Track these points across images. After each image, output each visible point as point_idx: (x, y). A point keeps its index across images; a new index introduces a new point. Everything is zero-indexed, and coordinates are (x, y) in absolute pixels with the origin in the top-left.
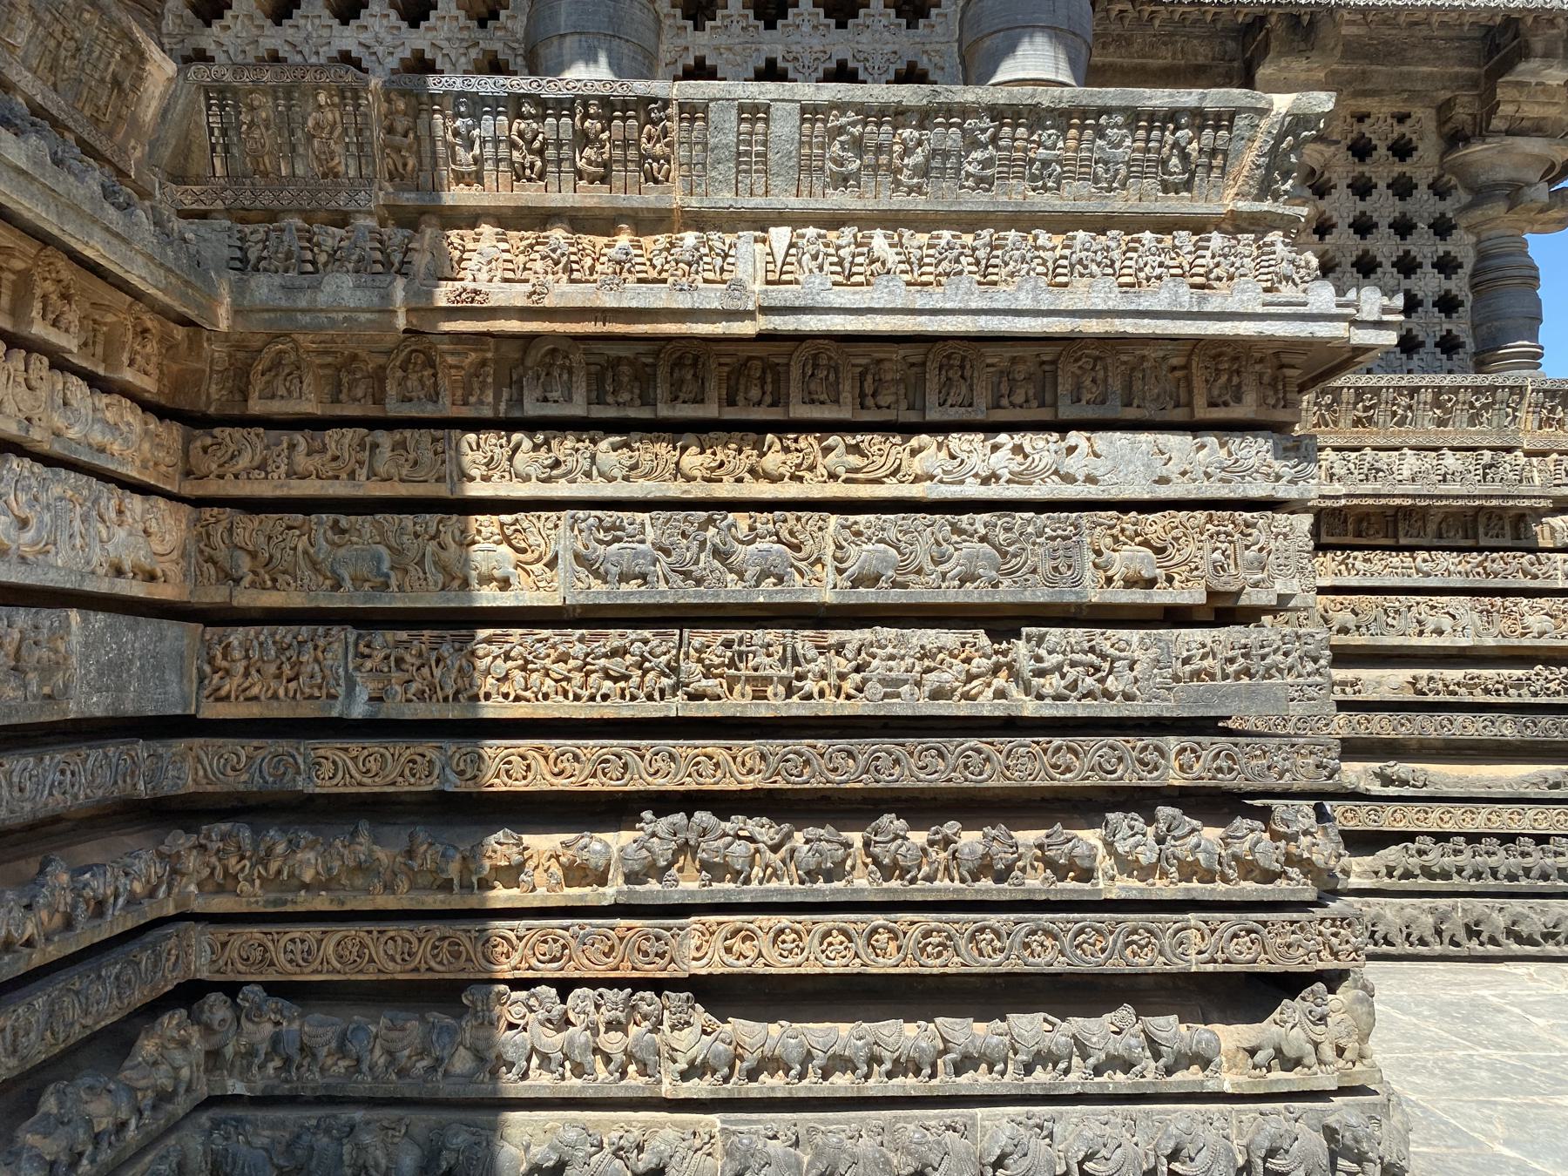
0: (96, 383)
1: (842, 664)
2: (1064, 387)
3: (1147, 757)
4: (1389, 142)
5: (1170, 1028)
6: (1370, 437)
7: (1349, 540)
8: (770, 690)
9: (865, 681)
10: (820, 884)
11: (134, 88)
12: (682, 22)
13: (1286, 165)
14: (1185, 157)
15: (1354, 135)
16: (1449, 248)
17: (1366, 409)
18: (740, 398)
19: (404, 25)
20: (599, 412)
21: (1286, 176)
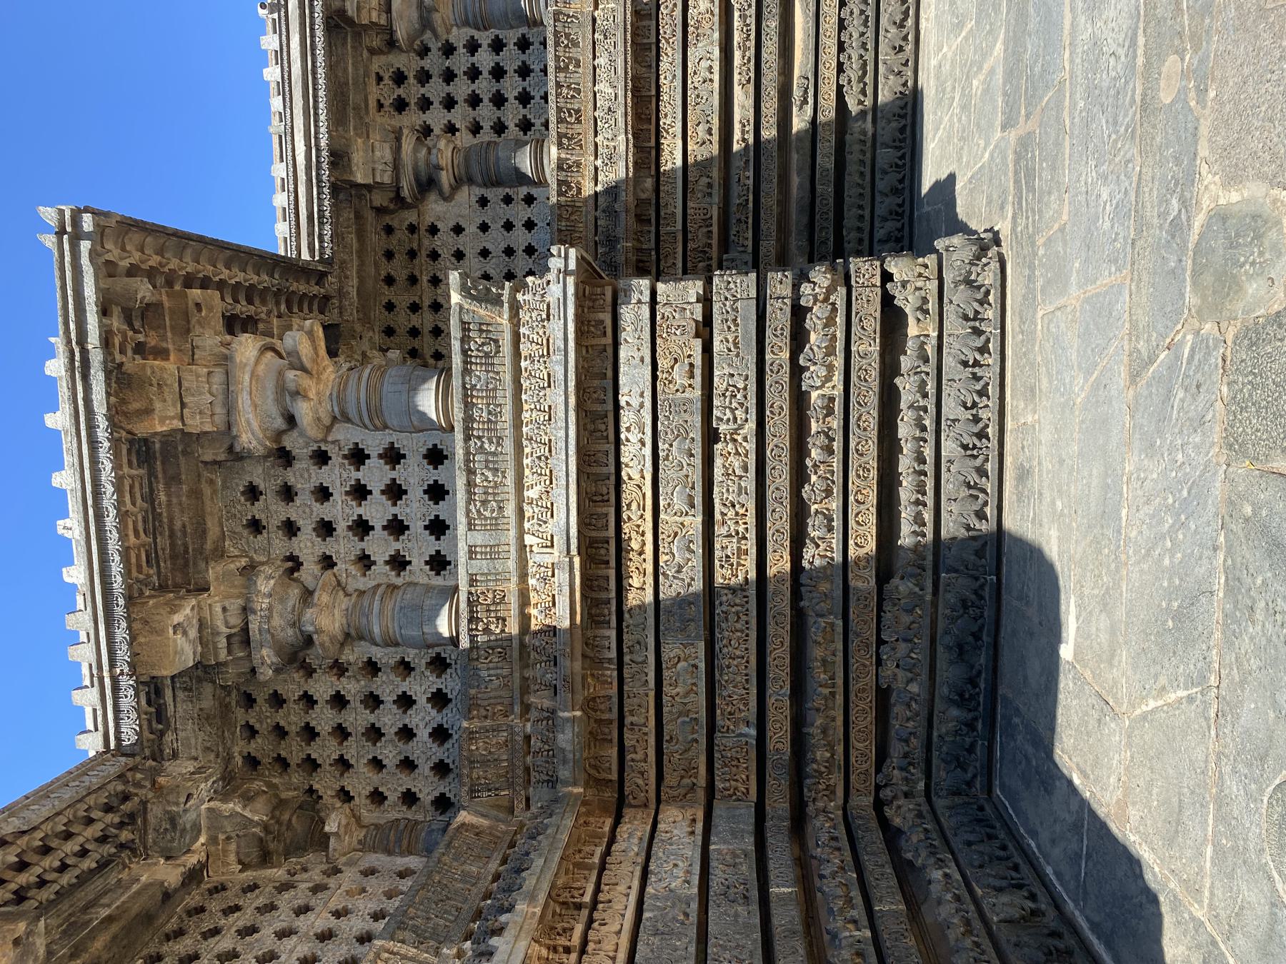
0: (612, 840)
1: (731, 513)
2: (599, 408)
3: (775, 369)
4: (395, 87)
5: (906, 362)
6: (588, 113)
7: (653, 127)
8: (743, 547)
9: (739, 503)
10: (834, 524)
11: (477, 828)
12: (408, 572)
14: (483, 344)
15: (392, 110)
16: (461, 45)
17: (570, 115)
18: (605, 558)
19: (415, 707)
20: (614, 623)
21: (489, 290)
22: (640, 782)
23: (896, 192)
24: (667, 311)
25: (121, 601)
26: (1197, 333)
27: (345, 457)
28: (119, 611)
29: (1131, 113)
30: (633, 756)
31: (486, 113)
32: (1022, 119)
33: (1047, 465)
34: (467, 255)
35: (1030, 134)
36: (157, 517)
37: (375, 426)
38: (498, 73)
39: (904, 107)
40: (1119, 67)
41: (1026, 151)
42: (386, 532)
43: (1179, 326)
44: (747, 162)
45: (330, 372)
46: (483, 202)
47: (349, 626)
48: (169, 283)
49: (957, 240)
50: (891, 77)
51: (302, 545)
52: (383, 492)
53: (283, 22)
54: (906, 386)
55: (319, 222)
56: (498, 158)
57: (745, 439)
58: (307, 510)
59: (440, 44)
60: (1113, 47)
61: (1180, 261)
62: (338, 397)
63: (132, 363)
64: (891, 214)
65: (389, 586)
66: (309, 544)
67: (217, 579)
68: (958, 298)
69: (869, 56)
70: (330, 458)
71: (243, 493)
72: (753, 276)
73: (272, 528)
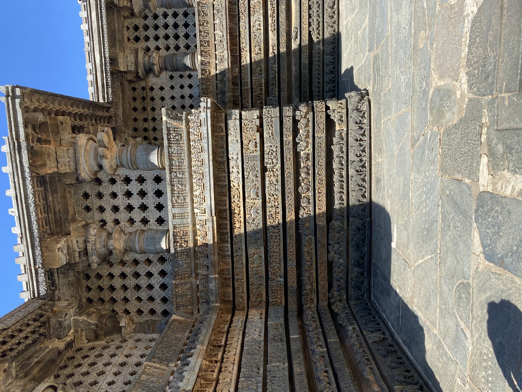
0: (231, 322)
1: (272, 198)
2: (221, 159)
3: (287, 144)
4: (135, 32)
5: (335, 140)
8: (277, 211)
9: (275, 194)
10: (311, 201)
11: (180, 321)
12: (148, 225)
13: (175, 115)
14: (176, 136)
17: (205, 43)
18: (225, 217)
19: (153, 277)
21: (177, 115)
22: (241, 300)
23: (332, 72)
24: (246, 122)
25: (38, 240)
26: (432, 130)
27: (122, 181)
28: (37, 243)
29: (410, 50)
30: (238, 291)
31: (172, 42)
32: (375, 49)
33: (386, 177)
34: (166, 98)
35: (378, 54)
36: (49, 206)
37: (134, 168)
38: (176, 26)
39: (334, 39)
40: (406, 33)
41: (377, 61)
42: (139, 210)
43: (426, 128)
44: (275, 61)
45: (116, 148)
46: (172, 77)
47: (126, 246)
48: (49, 114)
49: (353, 94)
50: (329, 28)
51: (107, 216)
52: (138, 194)
53: (88, 6)
54: (335, 149)
55: (107, 87)
56: (177, 60)
57: (277, 170)
58: (108, 202)
59: (152, 15)
60: (404, 25)
61: (426, 104)
62: (119, 157)
63: (37, 146)
64: (330, 81)
65: (141, 230)
66: (109, 215)
67: (73, 230)
68: (354, 115)
69: (321, 20)
70: (116, 181)
71: (82, 196)
72: (278, 108)
73: (94, 209)
